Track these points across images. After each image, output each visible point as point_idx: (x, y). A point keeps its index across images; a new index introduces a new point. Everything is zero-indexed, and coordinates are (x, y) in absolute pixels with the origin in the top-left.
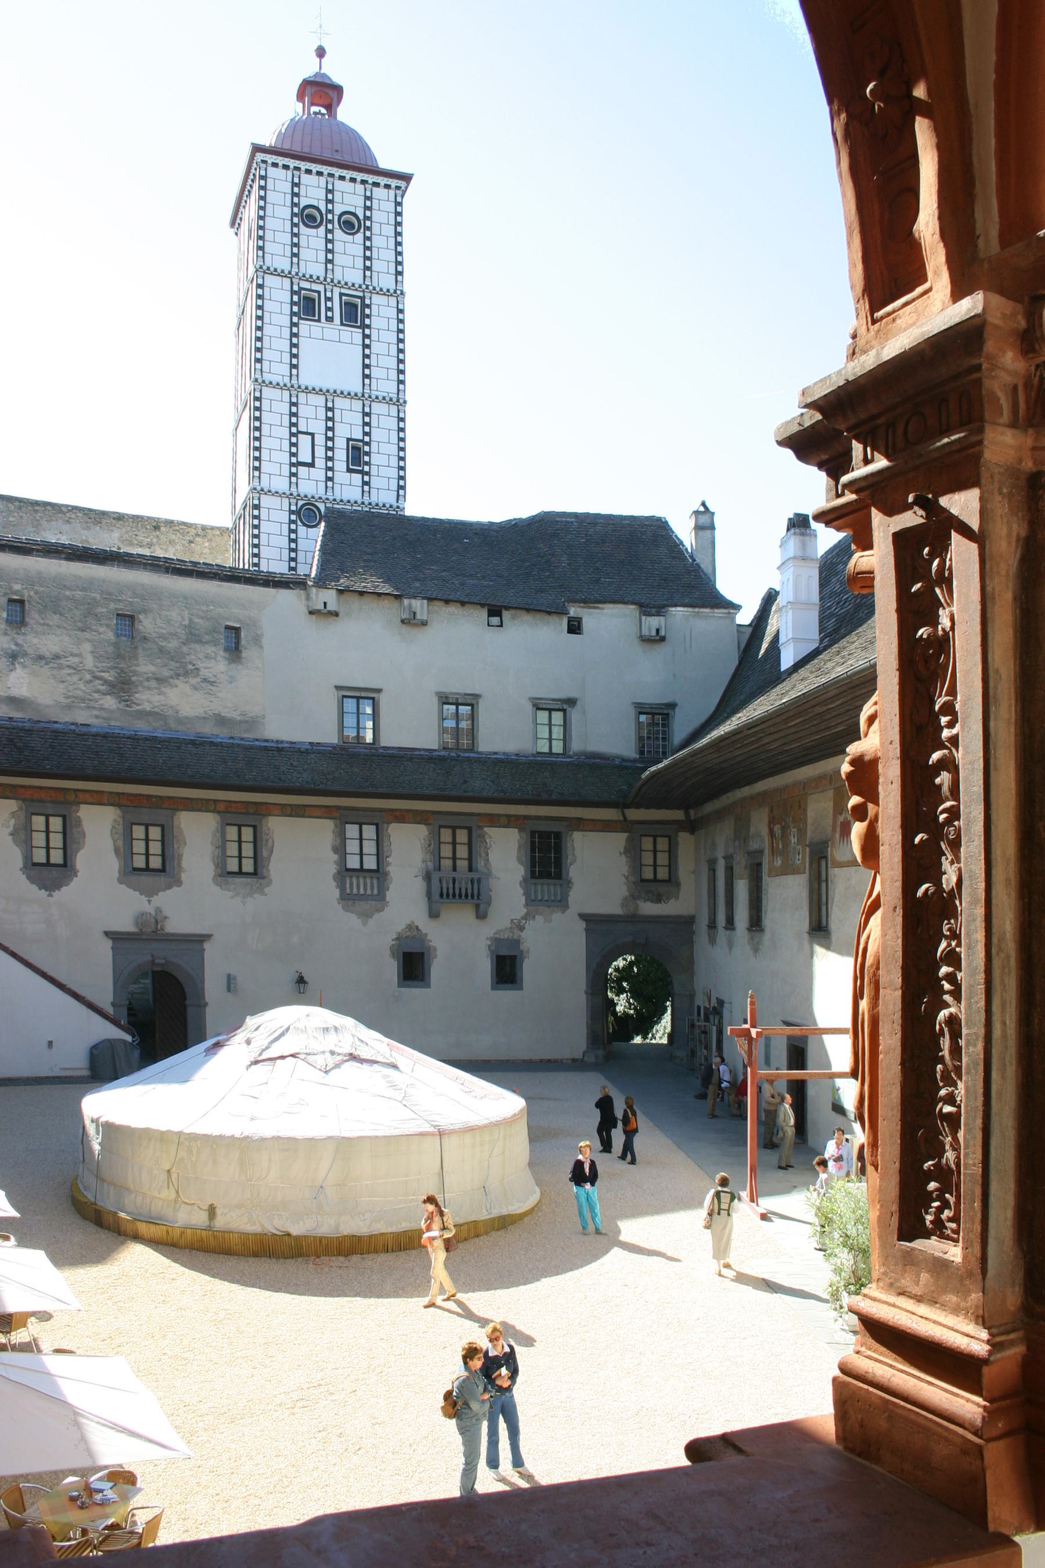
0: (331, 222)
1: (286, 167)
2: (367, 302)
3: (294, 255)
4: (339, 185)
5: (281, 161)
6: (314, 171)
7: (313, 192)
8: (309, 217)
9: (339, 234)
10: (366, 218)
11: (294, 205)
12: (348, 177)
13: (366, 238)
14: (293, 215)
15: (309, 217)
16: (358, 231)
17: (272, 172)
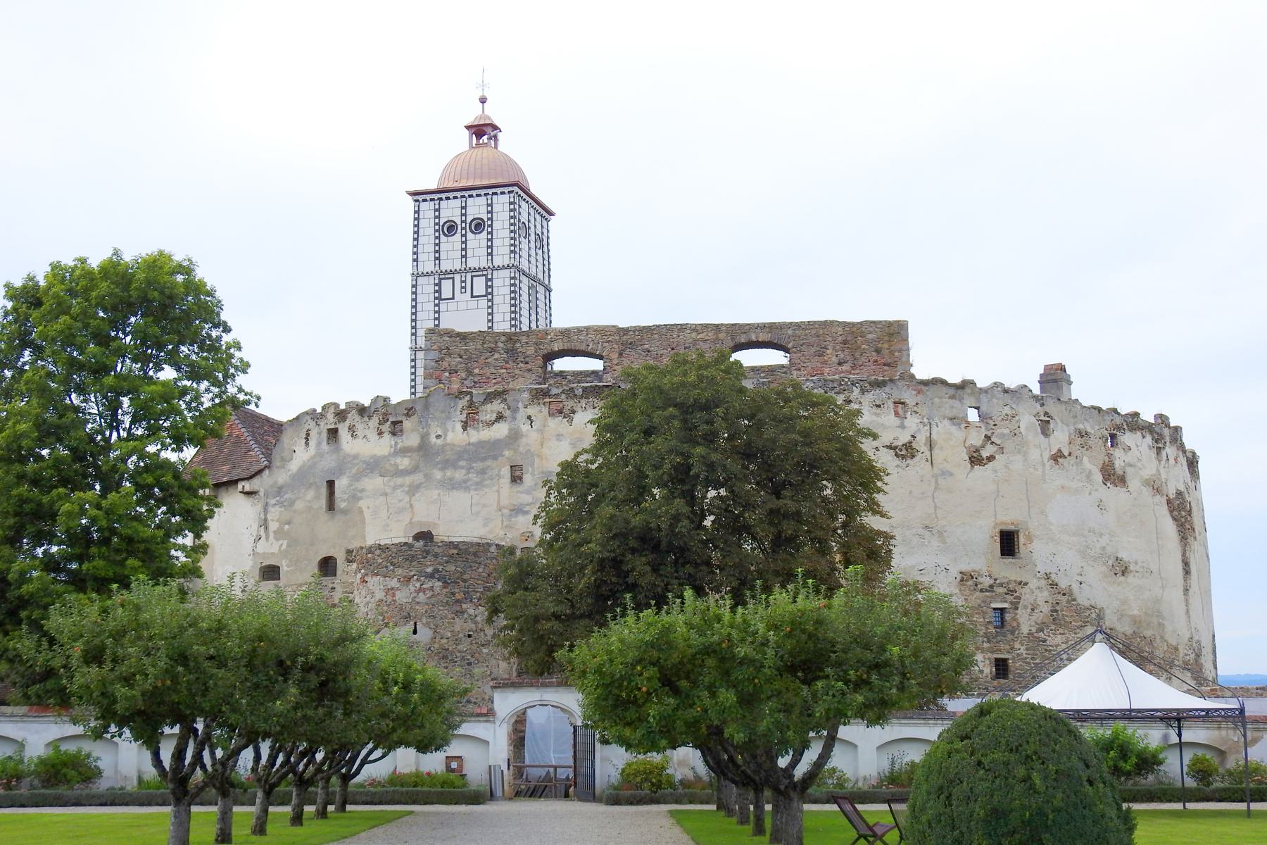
0: (462, 229)
1: (432, 200)
2: (490, 277)
3: (436, 259)
4: (470, 201)
5: (428, 197)
6: (451, 197)
7: (451, 210)
8: (451, 228)
9: (470, 235)
10: (489, 219)
11: (436, 224)
12: (482, 194)
13: (489, 233)
14: (436, 231)
15: (451, 228)
16: (483, 230)
17: (423, 206)
